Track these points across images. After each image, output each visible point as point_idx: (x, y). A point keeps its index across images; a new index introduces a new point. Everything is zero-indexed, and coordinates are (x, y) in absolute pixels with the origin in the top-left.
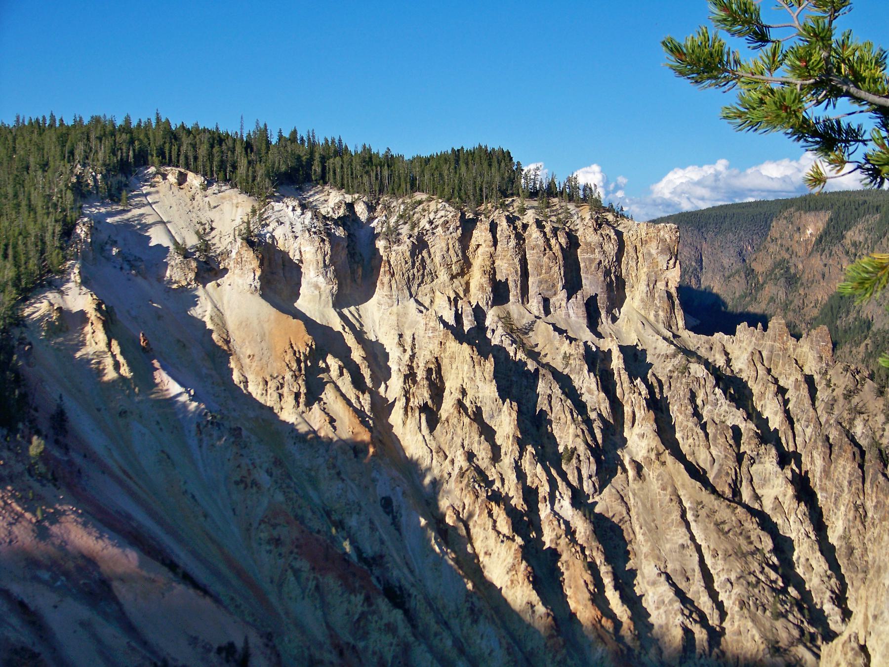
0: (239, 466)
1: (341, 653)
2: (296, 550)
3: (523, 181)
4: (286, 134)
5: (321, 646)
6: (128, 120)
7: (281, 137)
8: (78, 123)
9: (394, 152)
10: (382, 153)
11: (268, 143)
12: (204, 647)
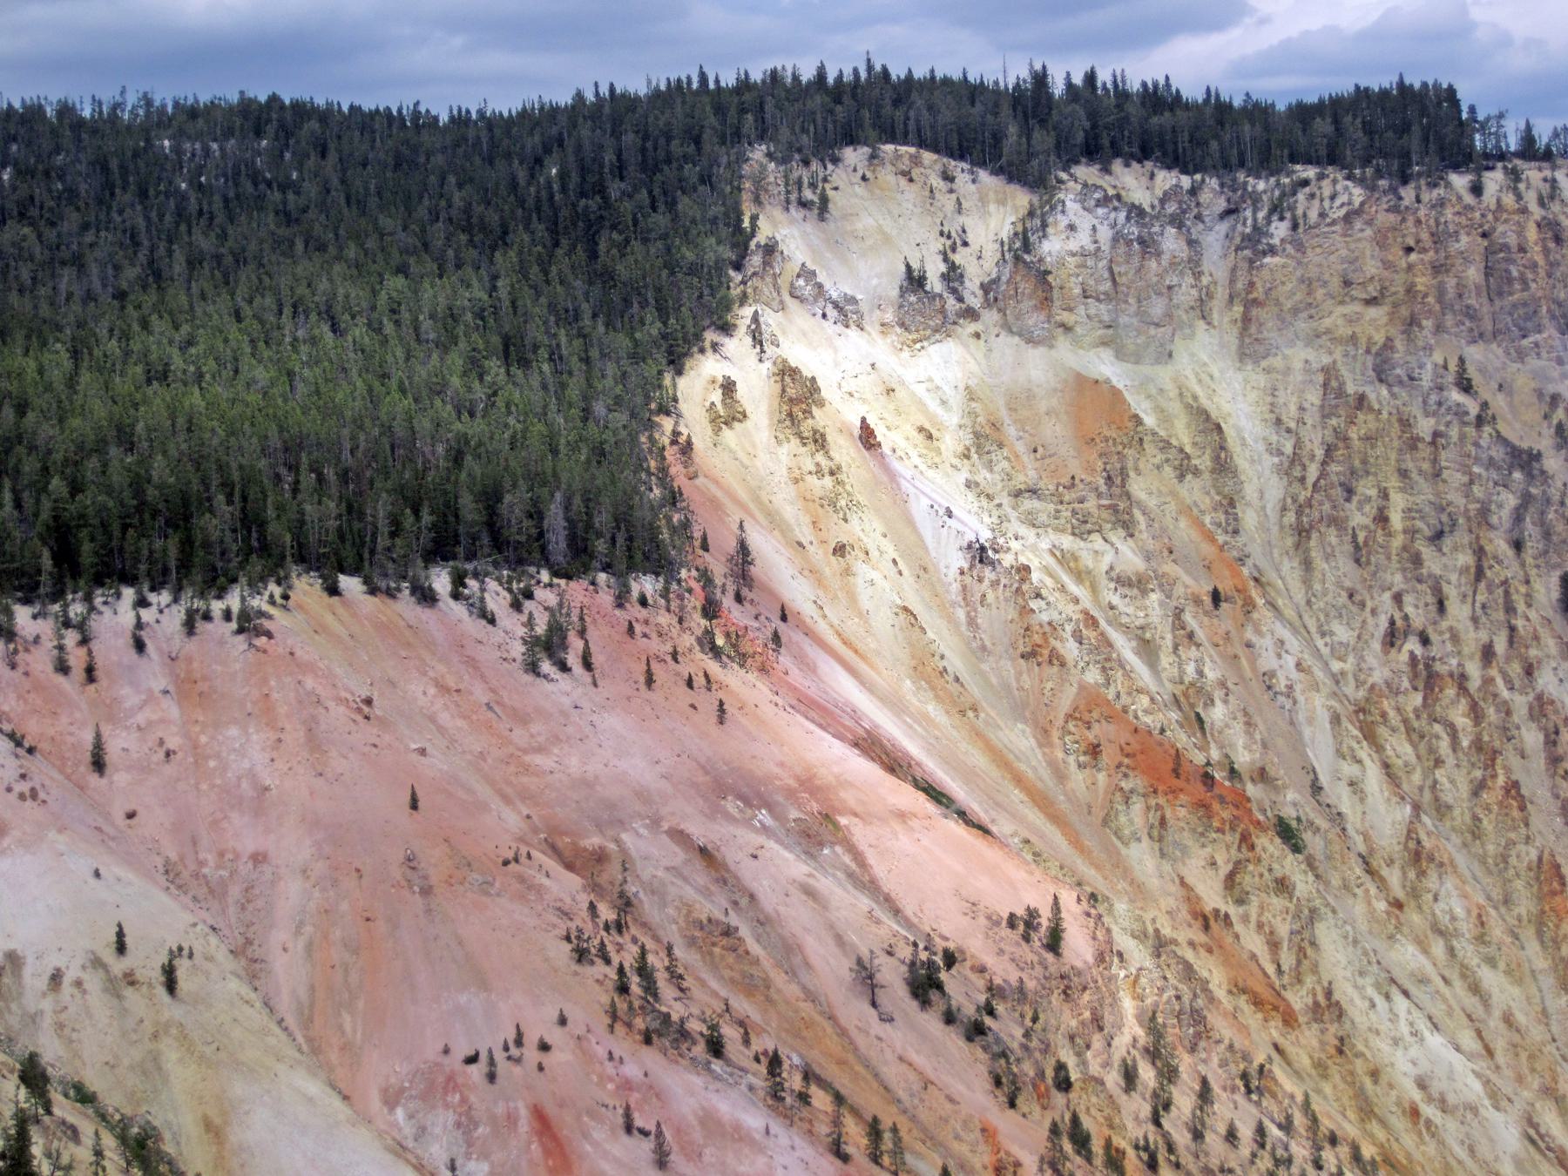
0: (1027, 629)
1: (1206, 927)
2: (1126, 761)
3: (1477, 136)
4: (1078, 80)
6: (821, 75)
7: (1069, 85)
8: (744, 85)
11: (1050, 96)
12: (989, 918)
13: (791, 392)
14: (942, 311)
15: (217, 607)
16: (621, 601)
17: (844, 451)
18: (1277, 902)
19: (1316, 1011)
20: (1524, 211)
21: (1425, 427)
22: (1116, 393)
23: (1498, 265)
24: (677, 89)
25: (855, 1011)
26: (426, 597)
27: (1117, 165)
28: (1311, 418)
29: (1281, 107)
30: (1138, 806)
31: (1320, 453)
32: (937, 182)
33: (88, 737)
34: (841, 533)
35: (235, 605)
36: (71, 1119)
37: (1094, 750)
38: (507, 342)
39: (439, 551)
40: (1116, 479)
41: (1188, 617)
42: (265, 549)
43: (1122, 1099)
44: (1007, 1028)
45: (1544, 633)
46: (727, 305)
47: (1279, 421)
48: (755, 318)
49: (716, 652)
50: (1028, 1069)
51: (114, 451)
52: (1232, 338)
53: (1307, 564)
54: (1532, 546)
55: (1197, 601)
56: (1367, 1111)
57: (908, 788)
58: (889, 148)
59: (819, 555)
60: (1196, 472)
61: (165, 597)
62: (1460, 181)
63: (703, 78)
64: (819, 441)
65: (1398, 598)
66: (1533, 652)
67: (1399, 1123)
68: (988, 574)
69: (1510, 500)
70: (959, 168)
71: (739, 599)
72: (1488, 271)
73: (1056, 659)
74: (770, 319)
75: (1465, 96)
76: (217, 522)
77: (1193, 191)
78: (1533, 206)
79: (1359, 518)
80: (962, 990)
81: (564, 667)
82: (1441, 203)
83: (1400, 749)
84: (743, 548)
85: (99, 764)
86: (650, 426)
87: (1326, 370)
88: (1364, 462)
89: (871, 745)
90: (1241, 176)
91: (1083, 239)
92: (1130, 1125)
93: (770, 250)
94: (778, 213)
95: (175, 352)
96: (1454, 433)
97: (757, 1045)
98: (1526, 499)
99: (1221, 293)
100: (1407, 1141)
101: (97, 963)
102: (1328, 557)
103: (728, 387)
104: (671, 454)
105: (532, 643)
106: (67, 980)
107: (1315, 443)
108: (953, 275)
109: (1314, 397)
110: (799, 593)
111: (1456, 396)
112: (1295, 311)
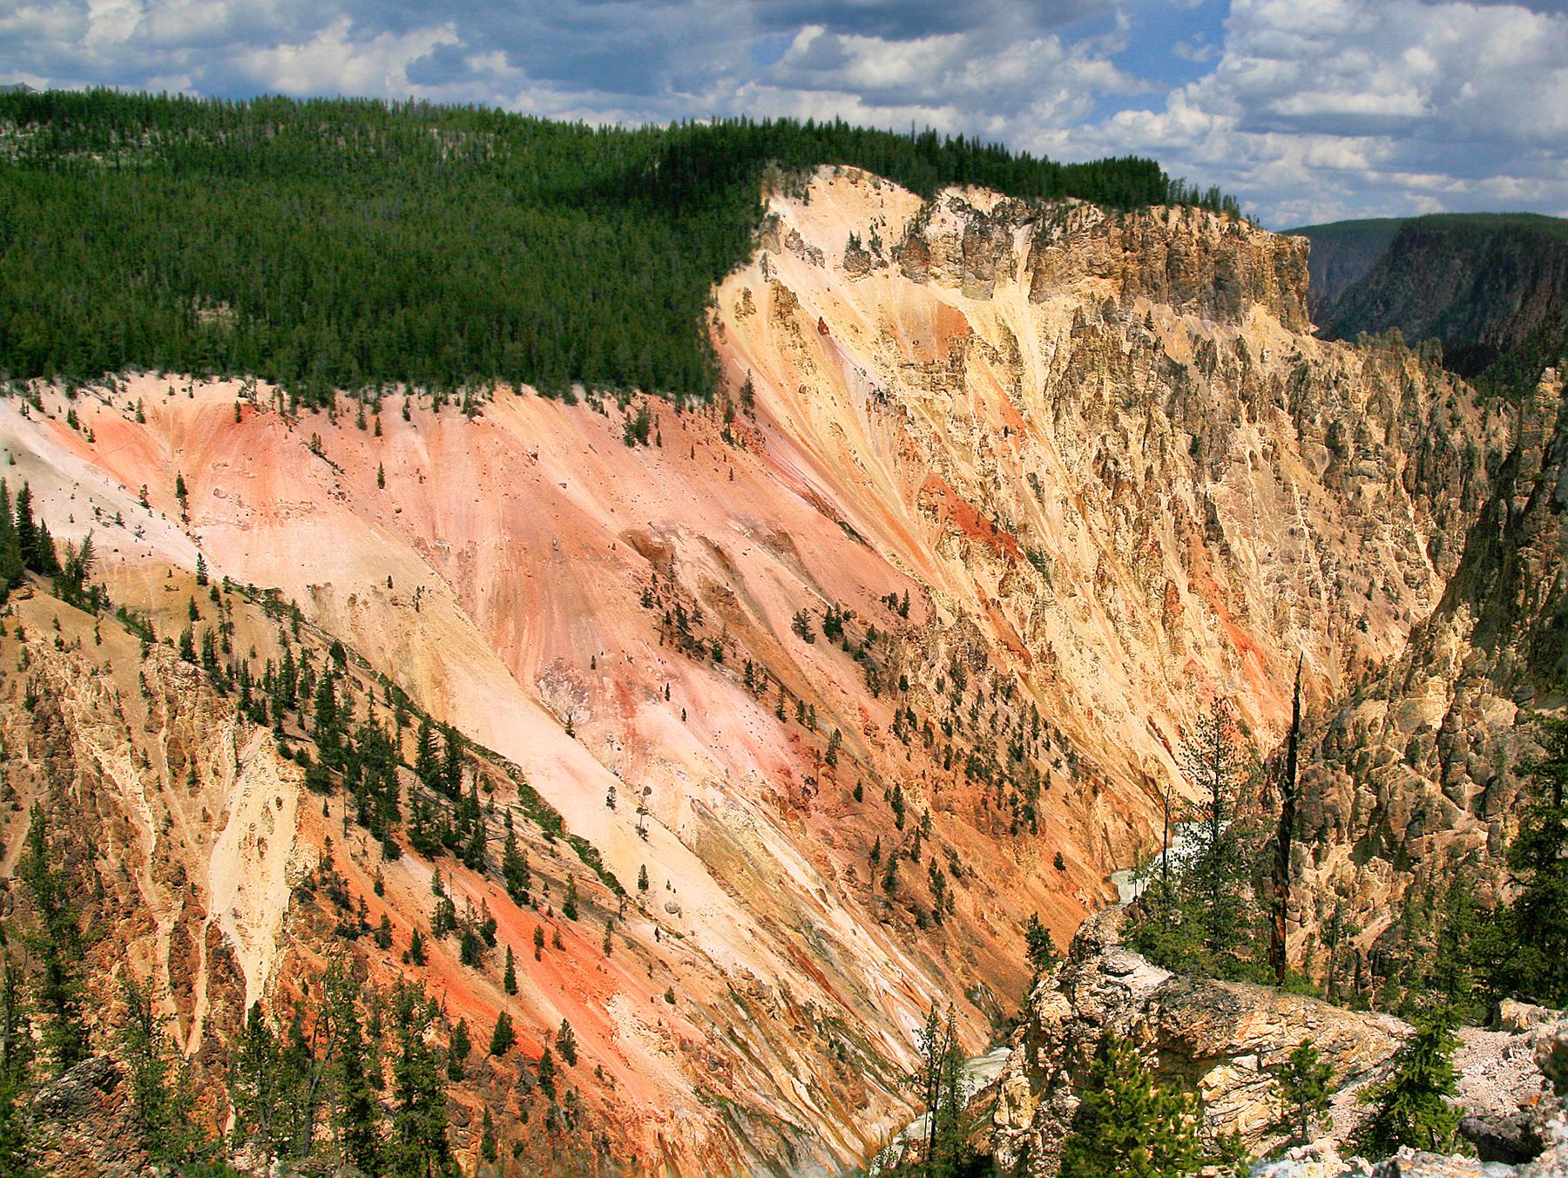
4: (953, 139)
5: (969, 599)
6: (811, 123)
7: (948, 141)
8: (767, 125)
10: (1040, 158)
13: (781, 300)
14: (869, 262)
15: (452, 397)
16: (679, 411)
17: (809, 335)
18: (1026, 597)
19: (1042, 658)
20: (1190, 234)
21: (1126, 347)
22: (961, 314)
23: (1174, 261)
25: (794, 642)
26: (571, 401)
27: (971, 187)
28: (1066, 335)
30: (955, 541)
31: (1068, 356)
32: (870, 187)
34: (806, 381)
35: (463, 399)
37: (934, 510)
38: (624, 259)
39: (576, 376)
40: (957, 361)
41: (990, 440)
43: (935, 697)
44: (877, 655)
46: (750, 248)
47: (1047, 338)
48: (765, 257)
49: (730, 441)
51: (398, 306)
52: (1027, 289)
53: (1057, 418)
54: (1179, 416)
55: (997, 433)
56: (1065, 711)
58: (846, 168)
59: (789, 392)
60: (1001, 362)
61: (423, 391)
62: (1157, 212)
63: (744, 119)
64: (796, 328)
65: (1104, 439)
66: (1173, 474)
67: (1084, 720)
68: (882, 408)
69: (1168, 391)
70: (885, 185)
71: (746, 412)
72: (1168, 265)
74: (773, 259)
75: (1163, 170)
76: (456, 348)
77: (1012, 206)
78: (1195, 232)
79: (1086, 393)
80: (854, 632)
81: (646, 444)
82: (1146, 225)
83: (1099, 519)
85: (381, 483)
87: (1076, 311)
88: (1092, 363)
89: (813, 499)
90: (1038, 200)
91: (948, 228)
92: (939, 710)
94: (781, 198)
95: (435, 251)
96: (1142, 351)
98: (1177, 391)
99: (1022, 264)
100: (1088, 731)
102: (1068, 413)
103: (747, 295)
104: (713, 330)
105: (629, 428)
106: (359, 601)
107: (1066, 349)
108: (876, 244)
109: (1068, 326)
110: (779, 412)
111: (1145, 332)
112: (1062, 277)
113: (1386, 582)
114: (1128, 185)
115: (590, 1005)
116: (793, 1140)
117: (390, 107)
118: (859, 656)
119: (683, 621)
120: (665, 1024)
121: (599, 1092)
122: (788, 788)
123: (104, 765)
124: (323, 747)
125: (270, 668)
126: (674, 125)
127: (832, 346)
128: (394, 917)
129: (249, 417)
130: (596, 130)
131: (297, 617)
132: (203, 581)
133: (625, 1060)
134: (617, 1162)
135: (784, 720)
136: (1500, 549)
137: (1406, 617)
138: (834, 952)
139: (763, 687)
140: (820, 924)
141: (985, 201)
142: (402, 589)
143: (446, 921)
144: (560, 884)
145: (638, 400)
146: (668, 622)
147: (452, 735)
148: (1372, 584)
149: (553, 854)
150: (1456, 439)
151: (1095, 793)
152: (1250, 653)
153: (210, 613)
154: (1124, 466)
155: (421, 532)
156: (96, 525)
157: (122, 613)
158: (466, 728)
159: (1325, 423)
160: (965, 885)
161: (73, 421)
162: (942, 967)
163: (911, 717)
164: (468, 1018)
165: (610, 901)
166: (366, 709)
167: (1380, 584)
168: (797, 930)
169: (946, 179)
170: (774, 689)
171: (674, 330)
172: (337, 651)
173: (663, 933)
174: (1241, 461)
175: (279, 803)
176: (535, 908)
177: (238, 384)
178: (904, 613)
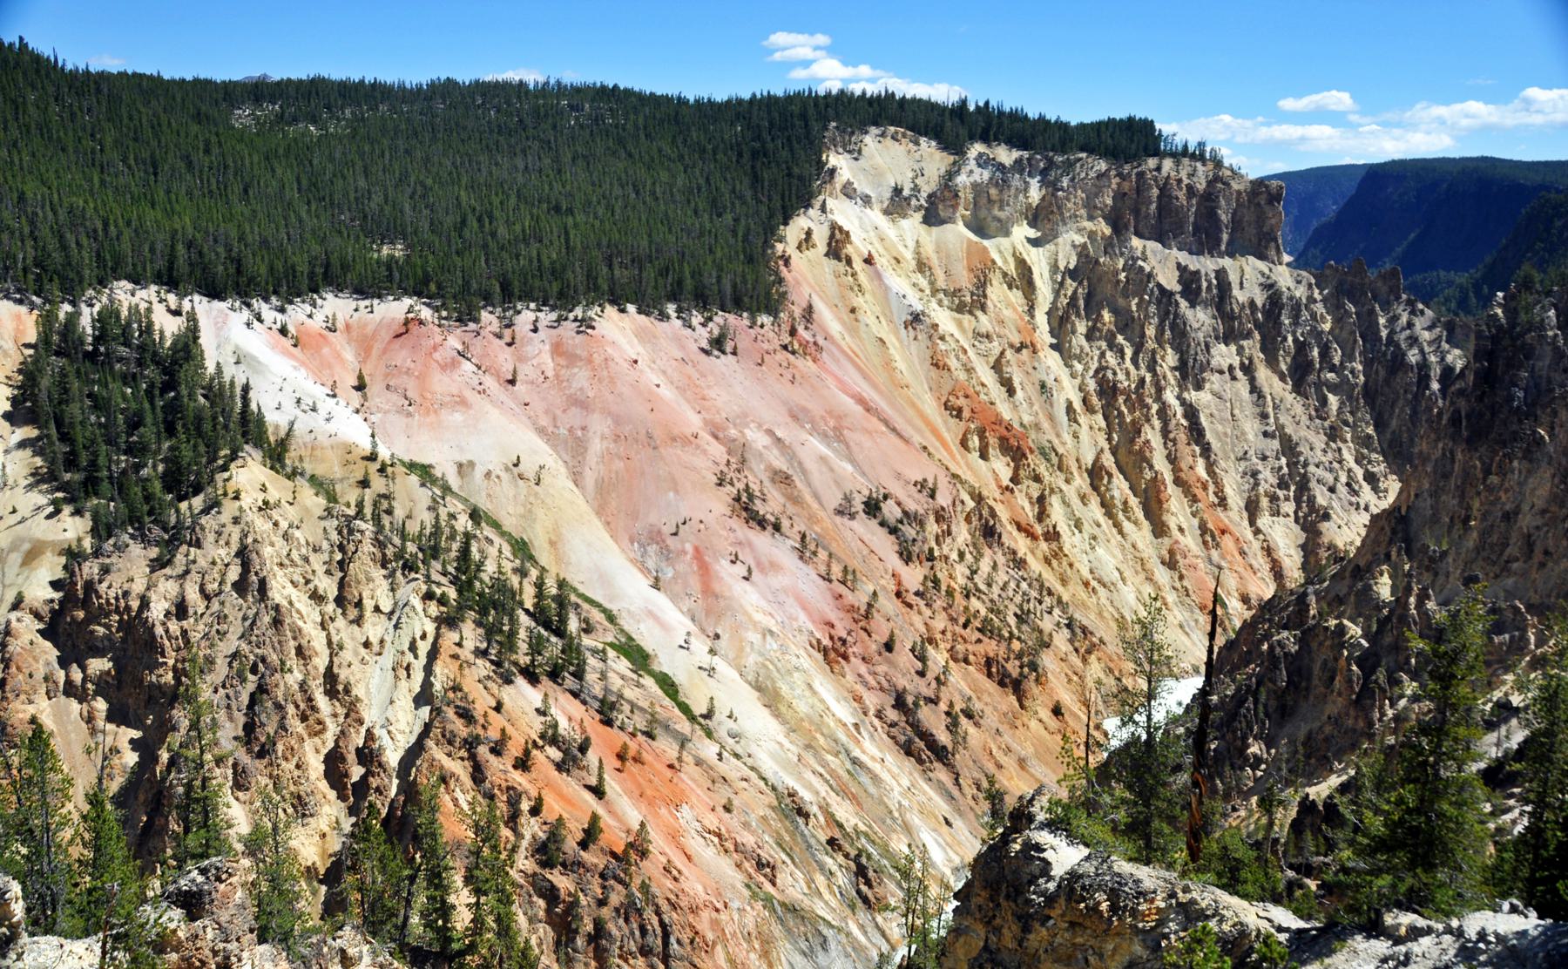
4: (981, 104)
6: (864, 93)
8: (828, 95)
9: (1064, 119)
18: (1036, 485)
24: (798, 95)
29: (1073, 123)
33: (511, 369)
36: (491, 536)
39: (673, 297)
42: (597, 288)
44: (910, 531)
45: (1169, 374)
49: (793, 353)
50: (916, 549)
57: (875, 420)
58: (892, 129)
62: (1152, 162)
70: (923, 140)
72: (1159, 208)
73: (946, 368)
74: (830, 203)
76: (576, 276)
80: (891, 511)
84: (810, 307)
86: (773, 247)
89: (861, 401)
91: (976, 177)
93: (833, 171)
97: (796, 528)
101: (507, 469)
103: (809, 233)
108: (916, 189)
111: (1140, 263)
113: (1349, 477)
114: (1130, 140)
115: (663, 811)
116: (825, 931)
117: (531, 87)
118: (893, 531)
119: (751, 497)
120: (723, 831)
121: (669, 883)
122: (831, 638)
123: (294, 599)
124: (460, 592)
125: (423, 528)
126: (754, 95)
127: (879, 276)
128: (510, 730)
129: (414, 328)
130: (692, 100)
131: (447, 489)
132: (372, 457)
133: (689, 858)
134: (679, 942)
135: (830, 581)
136: (1452, 453)
137: (1366, 509)
138: (865, 779)
139: (815, 553)
140: (856, 753)
141: (1006, 155)
142: (528, 467)
143: (551, 737)
144: (642, 709)
145: (719, 318)
146: (738, 499)
147: (562, 584)
148: (1336, 479)
149: (639, 685)
150: (1413, 357)
151: (1089, 652)
152: (1227, 536)
153: (378, 485)
154: (1121, 376)
155: (544, 421)
156: (298, 412)
157: (313, 480)
158: (574, 579)
159: (1296, 340)
160: (977, 725)
161: (283, 331)
162: (956, 793)
163: (936, 582)
164: (565, 815)
165: (684, 726)
166: (495, 560)
167: (1343, 479)
168: (836, 755)
169: (972, 138)
170: (823, 555)
171: (750, 260)
172: (475, 515)
173: (725, 754)
174: (1221, 372)
175: (424, 637)
176: (621, 728)
177: (407, 301)
178: (932, 496)
